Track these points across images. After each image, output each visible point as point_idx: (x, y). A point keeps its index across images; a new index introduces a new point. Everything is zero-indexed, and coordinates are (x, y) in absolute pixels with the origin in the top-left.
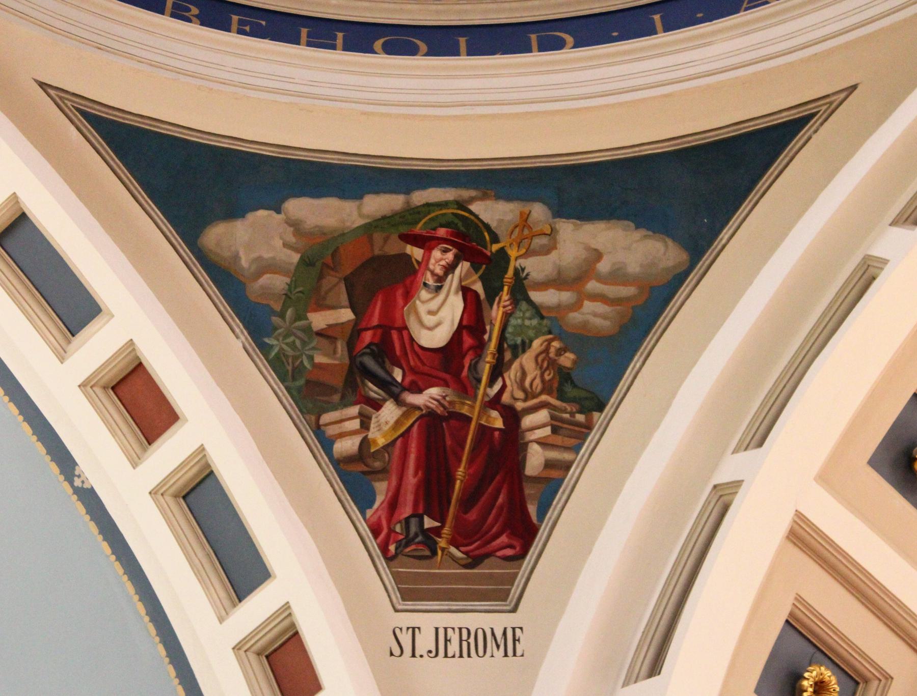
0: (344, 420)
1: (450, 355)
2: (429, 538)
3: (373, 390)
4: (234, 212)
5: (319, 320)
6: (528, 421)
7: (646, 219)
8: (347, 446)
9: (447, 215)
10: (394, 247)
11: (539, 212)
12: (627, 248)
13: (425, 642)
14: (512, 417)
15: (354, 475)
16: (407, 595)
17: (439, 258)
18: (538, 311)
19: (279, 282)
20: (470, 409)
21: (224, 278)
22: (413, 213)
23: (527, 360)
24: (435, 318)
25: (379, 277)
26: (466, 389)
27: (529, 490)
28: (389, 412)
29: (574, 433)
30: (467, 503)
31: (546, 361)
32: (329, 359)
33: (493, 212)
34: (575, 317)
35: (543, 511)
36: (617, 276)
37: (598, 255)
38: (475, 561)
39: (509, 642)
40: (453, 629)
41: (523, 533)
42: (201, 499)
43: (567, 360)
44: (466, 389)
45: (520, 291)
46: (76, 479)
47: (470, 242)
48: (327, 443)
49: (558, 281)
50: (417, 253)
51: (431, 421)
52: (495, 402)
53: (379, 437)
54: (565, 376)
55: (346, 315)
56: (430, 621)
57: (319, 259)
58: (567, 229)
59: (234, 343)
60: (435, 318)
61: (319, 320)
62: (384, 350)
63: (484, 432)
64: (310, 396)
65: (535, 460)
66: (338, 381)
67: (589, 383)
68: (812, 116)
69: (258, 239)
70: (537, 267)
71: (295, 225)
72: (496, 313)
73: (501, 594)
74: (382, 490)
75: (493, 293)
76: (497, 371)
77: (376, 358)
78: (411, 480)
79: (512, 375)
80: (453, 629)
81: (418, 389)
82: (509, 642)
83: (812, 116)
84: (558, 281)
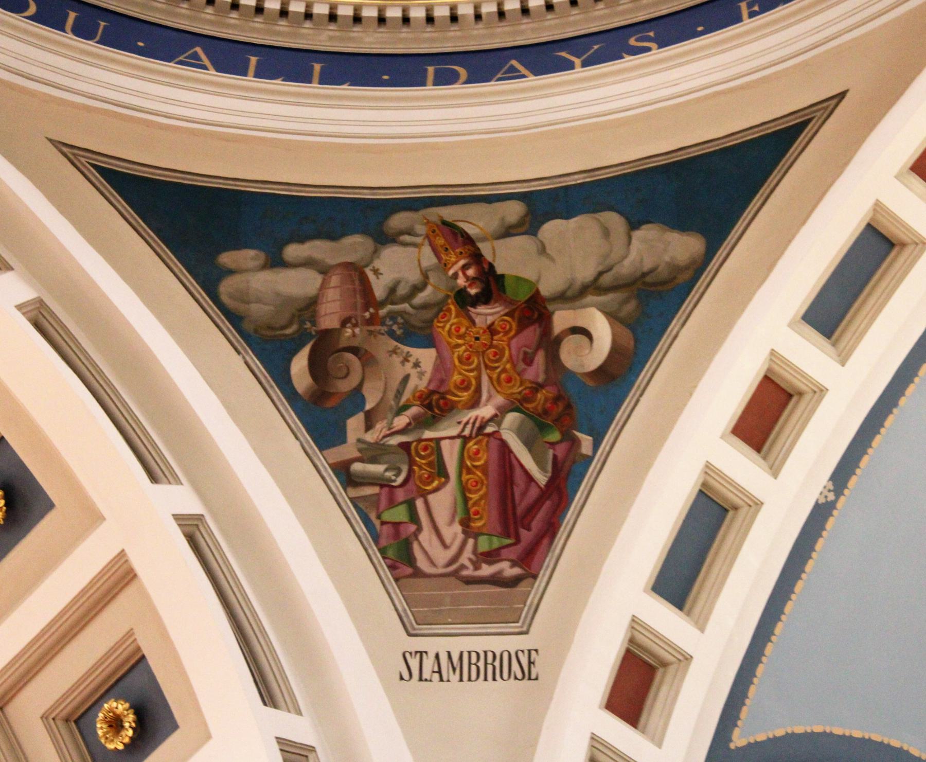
40: (523, 651)
46: (829, 499)
68: (95, 167)
80: (523, 651)
83: (95, 167)
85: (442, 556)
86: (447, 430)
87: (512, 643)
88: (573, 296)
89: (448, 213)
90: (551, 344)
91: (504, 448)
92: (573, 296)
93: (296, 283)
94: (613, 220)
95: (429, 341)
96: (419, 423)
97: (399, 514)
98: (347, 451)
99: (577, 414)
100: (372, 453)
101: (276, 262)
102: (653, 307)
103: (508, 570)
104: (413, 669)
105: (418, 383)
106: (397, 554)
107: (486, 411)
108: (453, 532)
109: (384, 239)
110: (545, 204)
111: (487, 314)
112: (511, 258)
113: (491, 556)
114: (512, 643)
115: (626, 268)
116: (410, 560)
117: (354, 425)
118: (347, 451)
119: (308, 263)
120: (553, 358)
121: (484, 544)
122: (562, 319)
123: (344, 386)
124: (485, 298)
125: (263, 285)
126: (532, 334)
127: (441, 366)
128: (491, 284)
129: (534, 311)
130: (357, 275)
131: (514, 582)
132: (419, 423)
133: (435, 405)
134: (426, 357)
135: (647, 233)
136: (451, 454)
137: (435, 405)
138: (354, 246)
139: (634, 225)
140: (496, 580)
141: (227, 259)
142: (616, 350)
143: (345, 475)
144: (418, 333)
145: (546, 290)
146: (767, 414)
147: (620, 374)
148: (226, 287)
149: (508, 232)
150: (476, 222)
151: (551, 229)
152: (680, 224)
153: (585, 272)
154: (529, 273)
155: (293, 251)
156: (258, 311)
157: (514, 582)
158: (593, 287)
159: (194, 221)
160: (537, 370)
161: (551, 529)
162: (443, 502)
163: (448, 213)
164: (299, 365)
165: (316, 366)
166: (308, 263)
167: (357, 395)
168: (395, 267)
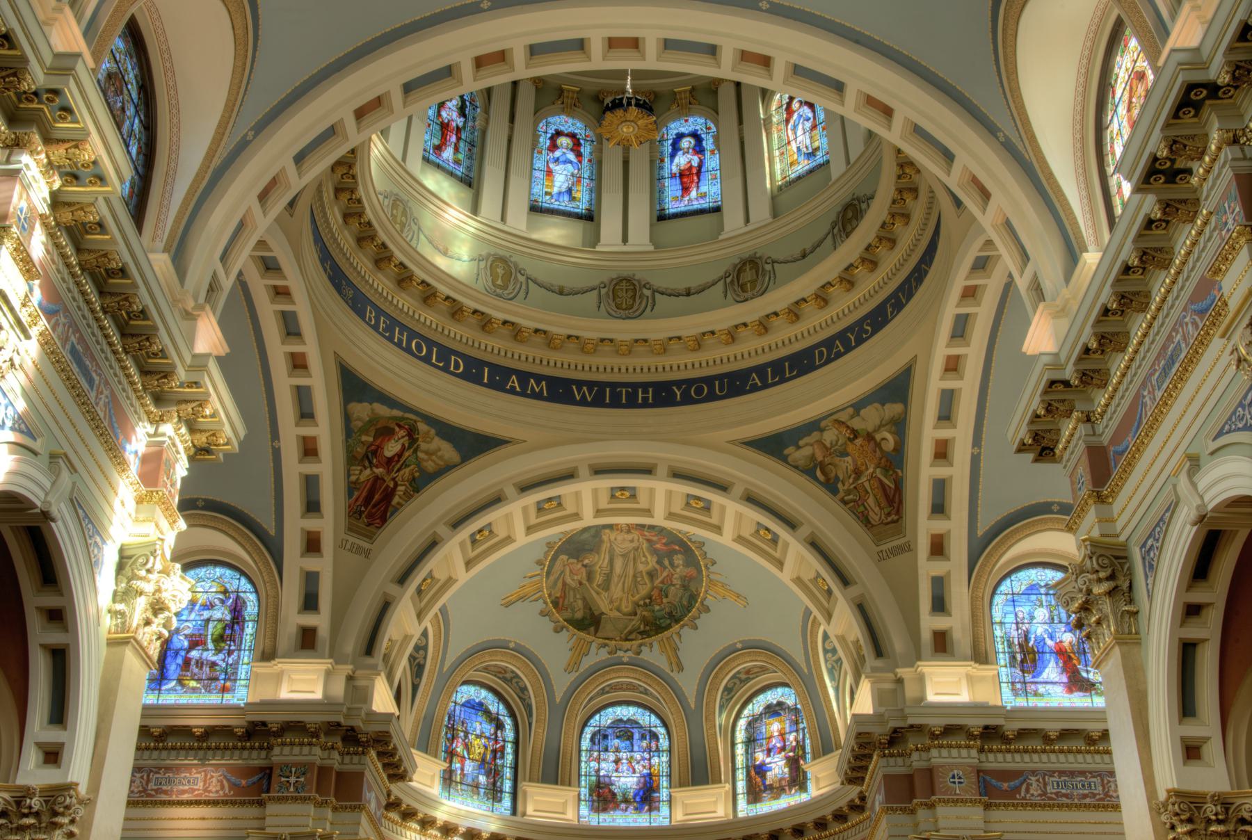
0: (356, 469)
1: (390, 461)
2: (361, 513)
3: (367, 464)
4: (360, 401)
5: (364, 438)
6: (400, 488)
7: (457, 447)
8: (353, 478)
9: (412, 423)
10: (393, 425)
11: (433, 432)
12: (448, 451)
13: (348, 546)
14: (396, 485)
15: (352, 487)
16: (350, 529)
17: (402, 433)
18: (417, 458)
19: (360, 424)
20: (387, 479)
21: (347, 418)
22: (403, 419)
23: (407, 470)
24: (392, 448)
25: (385, 432)
26: (389, 472)
27: (390, 509)
28: (368, 472)
29: (408, 497)
30: (374, 506)
31: (412, 473)
32: (360, 450)
33: (422, 427)
34: (425, 464)
35: (392, 515)
36: (441, 458)
37: (440, 450)
38: (369, 525)
39: (367, 553)
41: (384, 520)
42: (311, 484)
43: (417, 474)
44: (389, 472)
45: (416, 451)
47: (412, 433)
48: (349, 475)
49: (427, 453)
50: (397, 429)
51: (377, 479)
52: (394, 479)
53: (362, 478)
54: (414, 479)
55: (371, 439)
56: (353, 539)
57: (374, 420)
58: (437, 439)
59: (340, 437)
60: (392, 448)
61: (364, 438)
62: (375, 453)
63: (388, 486)
64: (351, 459)
65: (396, 500)
66: (359, 457)
67: (419, 483)
69: (362, 411)
70: (423, 446)
71: (372, 410)
72: (407, 454)
73: (370, 537)
74: (356, 494)
75: (409, 448)
76: (398, 470)
77: (371, 455)
78: (364, 494)
79: (402, 472)
81: (377, 467)
82: (367, 553)
84: (427, 453)
85: (877, 518)
86: (863, 479)
87: (902, 541)
88: (877, 430)
89: (835, 417)
90: (878, 445)
91: (880, 481)
92: (877, 430)
93: (807, 451)
94: (877, 405)
95: (847, 455)
96: (856, 479)
97: (862, 509)
98: (841, 494)
99: (894, 462)
100: (848, 492)
101: (799, 448)
102: (899, 425)
103: (896, 518)
104: (881, 557)
105: (851, 467)
106: (866, 522)
107: (871, 470)
108: (877, 509)
109: (822, 430)
110: (858, 406)
111: (859, 441)
112: (856, 424)
113: (889, 514)
114: (902, 541)
115: (887, 417)
116: (869, 522)
117: (840, 485)
118: (841, 494)
119: (807, 445)
120: (881, 449)
121: (886, 511)
122: (878, 437)
123: (833, 475)
124: (856, 437)
125: (799, 455)
126: (872, 443)
127: (854, 461)
128: (855, 434)
129: (870, 437)
130: (820, 442)
131: (897, 521)
132: (856, 479)
133: (858, 473)
134: (849, 459)
135: (887, 406)
136: (867, 485)
137: (858, 473)
138: (815, 436)
139: (883, 405)
140: (893, 522)
141: (786, 452)
142: (896, 443)
143: (845, 503)
144: (844, 454)
145: (870, 429)
146: (942, 452)
147: (900, 449)
148: (790, 459)
149: (852, 417)
150: (843, 417)
151: (862, 412)
152: (894, 402)
153: (877, 422)
154: (863, 427)
155: (801, 443)
156: (801, 463)
157: (897, 521)
158: (881, 426)
159: (773, 446)
160: (878, 453)
161: (901, 502)
162: (871, 501)
163: (835, 417)
164: (818, 473)
165: (823, 472)
166: (807, 445)
167: (837, 477)
168: (829, 436)
